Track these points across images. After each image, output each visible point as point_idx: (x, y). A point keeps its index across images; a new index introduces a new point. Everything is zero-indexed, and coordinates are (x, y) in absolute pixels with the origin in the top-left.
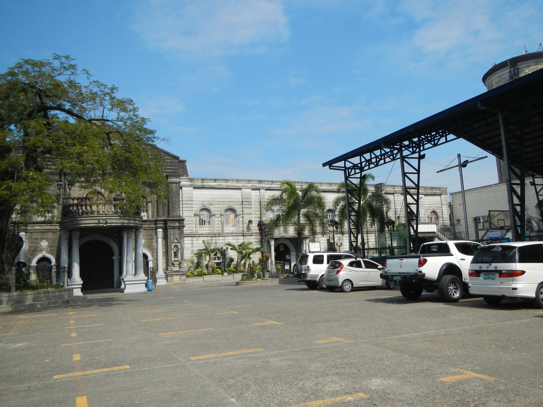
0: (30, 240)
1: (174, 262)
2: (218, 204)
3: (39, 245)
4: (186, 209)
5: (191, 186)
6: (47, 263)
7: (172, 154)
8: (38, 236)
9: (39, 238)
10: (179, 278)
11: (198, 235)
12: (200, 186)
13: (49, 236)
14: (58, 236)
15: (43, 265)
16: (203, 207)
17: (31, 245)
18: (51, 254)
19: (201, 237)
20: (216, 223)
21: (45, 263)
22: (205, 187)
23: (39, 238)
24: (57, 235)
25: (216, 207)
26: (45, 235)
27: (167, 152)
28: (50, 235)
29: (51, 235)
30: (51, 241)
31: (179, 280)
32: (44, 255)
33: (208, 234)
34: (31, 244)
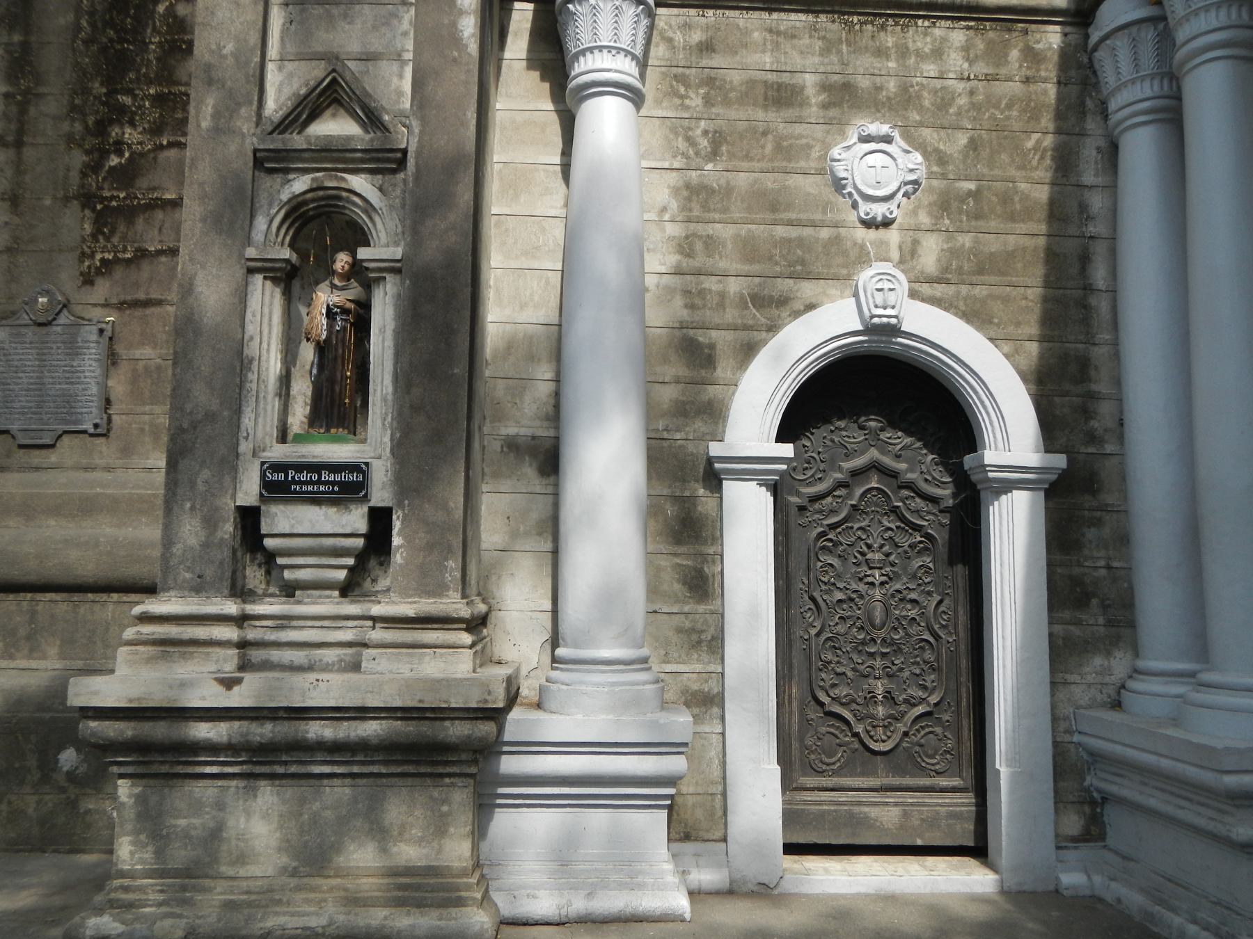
0: (696, 101)
3: (808, 185)
6: (900, 440)
8: (797, 61)
9: (809, 80)
13: (930, 69)
14: (1050, 71)
15: (856, 474)
17: (712, 172)
18: (974, 315)
21: (873, 439)
23: (809, 80)
24: (1032, 56)
26: (881, 52)
28: (938, 53)
29: (955, 61)
30: (962, 139)
32: (883, 316)
34: (714, 154)
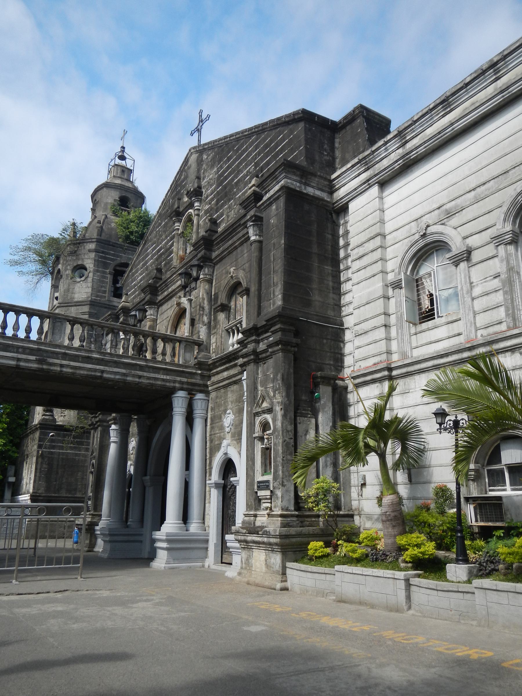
1: (259, 488)
2: (477, 201)
4: (362, 274)
5: (367, 184)
7: (287, 116)
10: (266, 561)
11: (404, 370)
12: (397, 166)
16: (421, 243)
19: (417, 377)
20: (477, 291)
22: (413, 155)
25: (470, 217)
27: (278, 119)
31: (264, 569)
33: (442, 356)
